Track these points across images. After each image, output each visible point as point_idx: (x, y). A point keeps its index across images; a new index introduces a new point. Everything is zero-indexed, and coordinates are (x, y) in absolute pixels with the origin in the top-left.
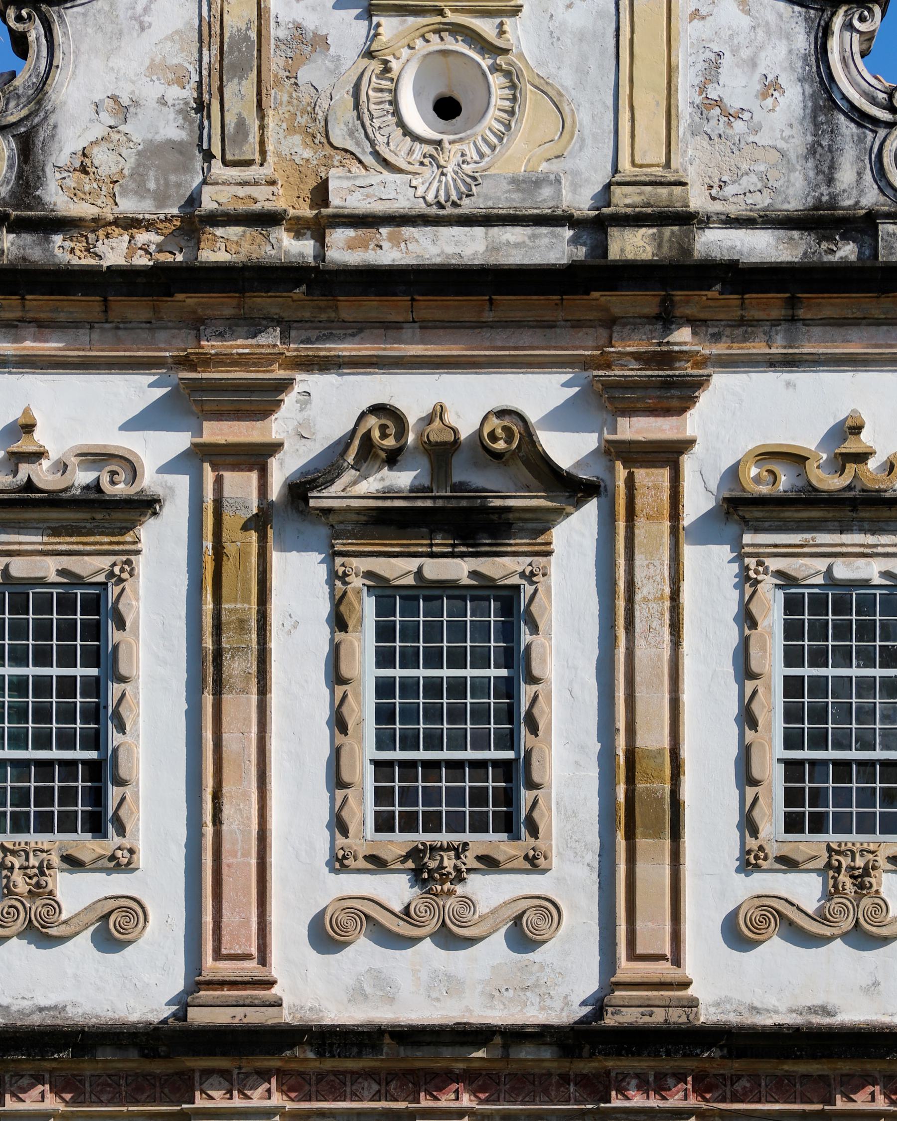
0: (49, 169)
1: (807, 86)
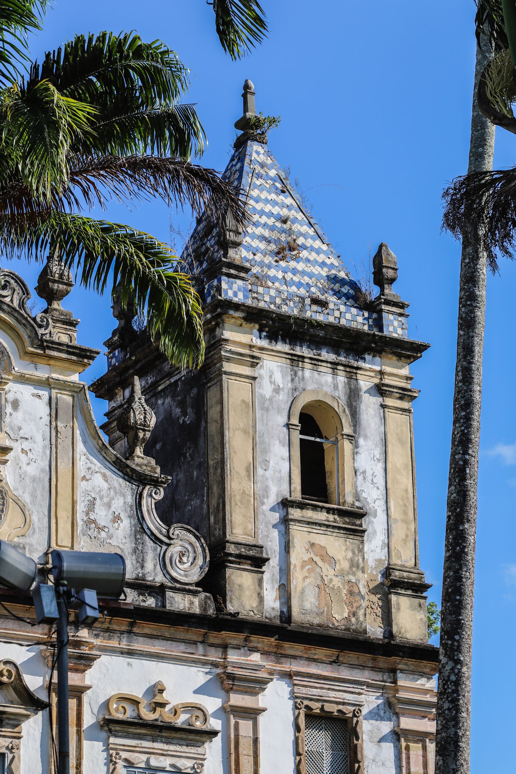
1: (132, 520)
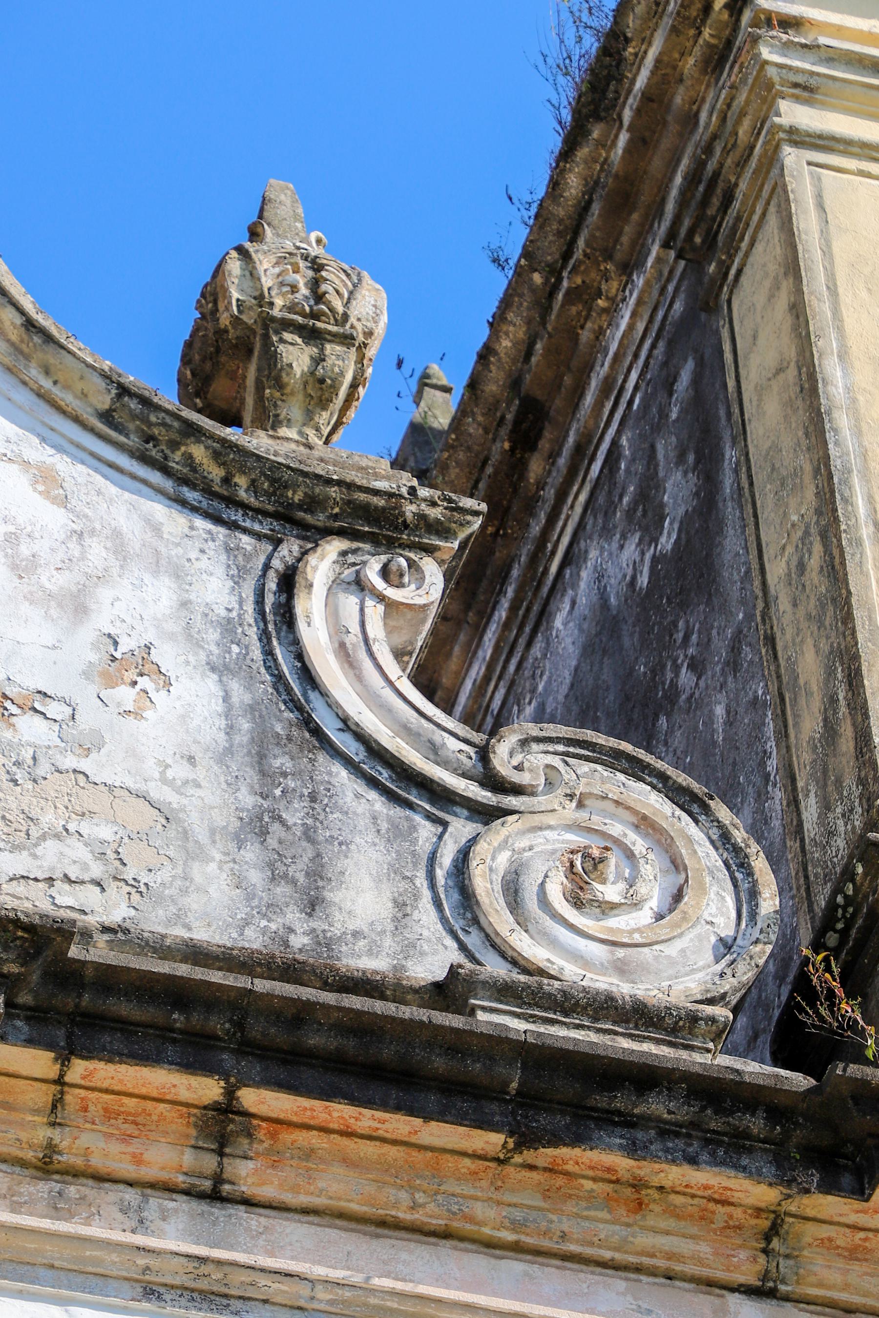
1: (235, 686)
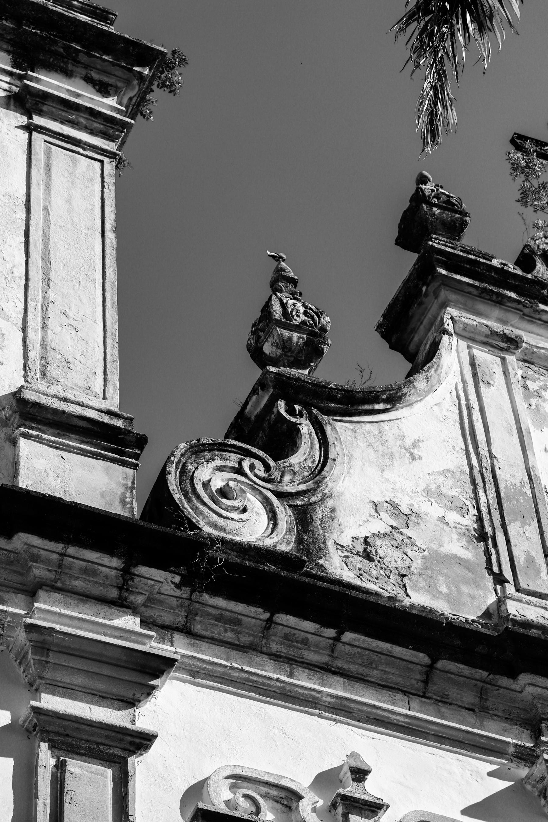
0: (330, 544)
